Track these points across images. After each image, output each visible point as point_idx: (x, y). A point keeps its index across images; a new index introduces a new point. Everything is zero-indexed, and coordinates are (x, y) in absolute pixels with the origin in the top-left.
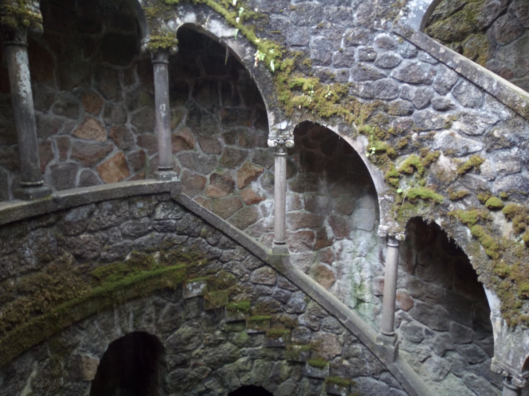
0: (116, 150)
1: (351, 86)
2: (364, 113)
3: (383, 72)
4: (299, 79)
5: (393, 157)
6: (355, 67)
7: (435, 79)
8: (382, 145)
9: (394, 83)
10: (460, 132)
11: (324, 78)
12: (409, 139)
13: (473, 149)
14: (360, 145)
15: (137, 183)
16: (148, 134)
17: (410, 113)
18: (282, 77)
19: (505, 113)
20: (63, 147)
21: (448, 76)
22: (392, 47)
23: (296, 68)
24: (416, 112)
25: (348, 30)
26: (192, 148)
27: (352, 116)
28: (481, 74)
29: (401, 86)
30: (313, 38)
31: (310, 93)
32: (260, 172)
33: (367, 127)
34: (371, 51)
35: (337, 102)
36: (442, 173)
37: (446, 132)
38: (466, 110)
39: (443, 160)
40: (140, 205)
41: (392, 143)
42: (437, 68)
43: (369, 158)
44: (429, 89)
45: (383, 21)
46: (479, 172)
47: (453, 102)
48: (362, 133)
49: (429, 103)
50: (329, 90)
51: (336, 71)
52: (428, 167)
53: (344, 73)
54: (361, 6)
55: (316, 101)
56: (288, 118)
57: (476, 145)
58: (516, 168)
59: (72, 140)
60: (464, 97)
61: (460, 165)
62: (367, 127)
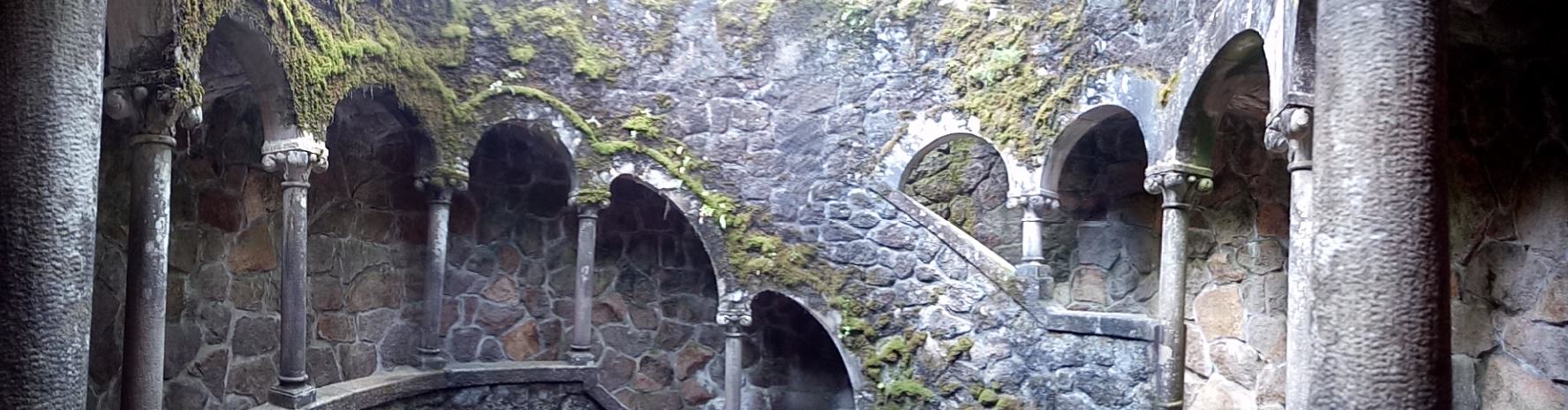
0: (528, 317)
1: (822, 247)
2: (837, 280)
3: (859, 232)
4: (757, 238)
5: (873, 340)
6: (825, 224)
7: (917, 243)
8: (859, 323)
9: (872, 246)
10: (948, 308)
11: (788, 236)
12: (891, 316)
13: (961, 330)
14: (832, 322)
15: (542, 365)
16: (567, 299)
17: (891, 283)
18: (735, 235)
19: (991, 288)
20: (470, 310)
21: (931, 242)
22: (869, 205)
23: (753, 224)
24: (899, 282)
25: (817, 183)
26: (620, 320)
27: (823, 284)
28: (962, 242)
29: (880, 250)
30: (775, 190)
31: (769, 255)
32: (710, 357)
33: (839, 299)
34: (845, 208)
35: (805, 267)
36: (931, 360)
37: (932, 308)
38: (952, 282)
39: (931, 344)
40: (543, 395)
41: (872, 320)
42: (918, 231)
43: (843, 341)
44: (911, 255)
45: (858, 175)
46: (969, 359)
47: (938, 272)
48: (834, 306)
49: (911, 274)
50: (794, 251)
51: (802, 229)
52: (914, 352)
53: (812, 231)
54: (833, 156)
55: (779, 266)
56: (743, 287)
57: (964, 325)
58: (1006, 351)
59: (481, 301)
60: (948, 267)
61: (950, 349)
62: (839, 299)
